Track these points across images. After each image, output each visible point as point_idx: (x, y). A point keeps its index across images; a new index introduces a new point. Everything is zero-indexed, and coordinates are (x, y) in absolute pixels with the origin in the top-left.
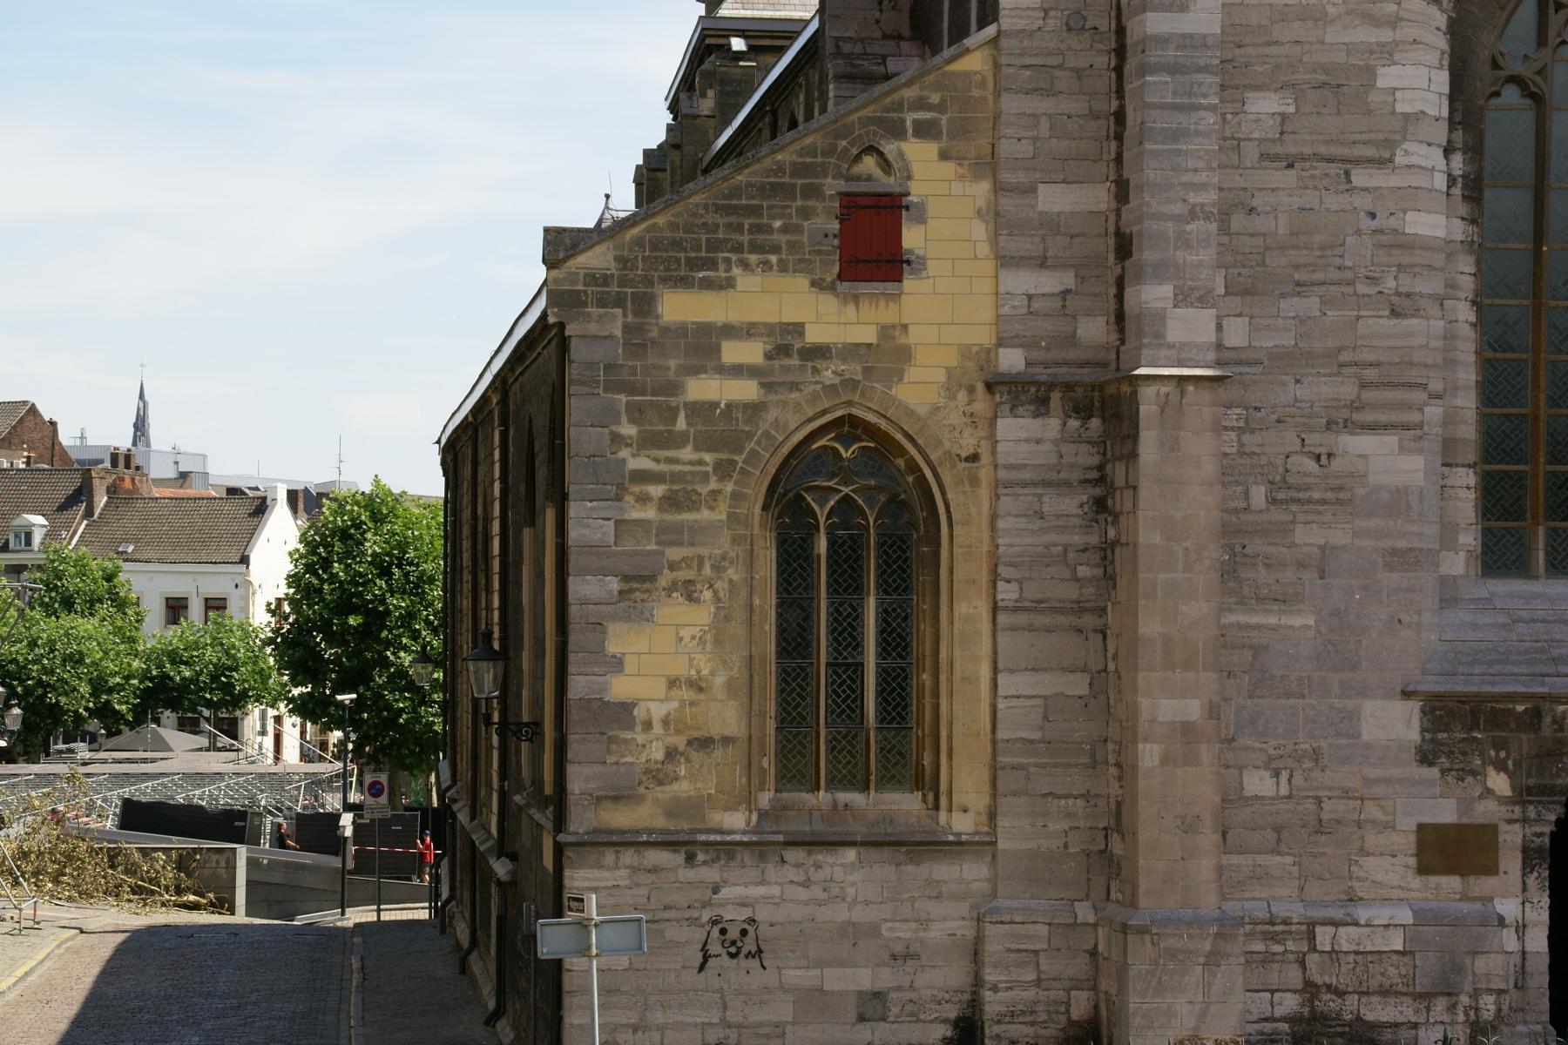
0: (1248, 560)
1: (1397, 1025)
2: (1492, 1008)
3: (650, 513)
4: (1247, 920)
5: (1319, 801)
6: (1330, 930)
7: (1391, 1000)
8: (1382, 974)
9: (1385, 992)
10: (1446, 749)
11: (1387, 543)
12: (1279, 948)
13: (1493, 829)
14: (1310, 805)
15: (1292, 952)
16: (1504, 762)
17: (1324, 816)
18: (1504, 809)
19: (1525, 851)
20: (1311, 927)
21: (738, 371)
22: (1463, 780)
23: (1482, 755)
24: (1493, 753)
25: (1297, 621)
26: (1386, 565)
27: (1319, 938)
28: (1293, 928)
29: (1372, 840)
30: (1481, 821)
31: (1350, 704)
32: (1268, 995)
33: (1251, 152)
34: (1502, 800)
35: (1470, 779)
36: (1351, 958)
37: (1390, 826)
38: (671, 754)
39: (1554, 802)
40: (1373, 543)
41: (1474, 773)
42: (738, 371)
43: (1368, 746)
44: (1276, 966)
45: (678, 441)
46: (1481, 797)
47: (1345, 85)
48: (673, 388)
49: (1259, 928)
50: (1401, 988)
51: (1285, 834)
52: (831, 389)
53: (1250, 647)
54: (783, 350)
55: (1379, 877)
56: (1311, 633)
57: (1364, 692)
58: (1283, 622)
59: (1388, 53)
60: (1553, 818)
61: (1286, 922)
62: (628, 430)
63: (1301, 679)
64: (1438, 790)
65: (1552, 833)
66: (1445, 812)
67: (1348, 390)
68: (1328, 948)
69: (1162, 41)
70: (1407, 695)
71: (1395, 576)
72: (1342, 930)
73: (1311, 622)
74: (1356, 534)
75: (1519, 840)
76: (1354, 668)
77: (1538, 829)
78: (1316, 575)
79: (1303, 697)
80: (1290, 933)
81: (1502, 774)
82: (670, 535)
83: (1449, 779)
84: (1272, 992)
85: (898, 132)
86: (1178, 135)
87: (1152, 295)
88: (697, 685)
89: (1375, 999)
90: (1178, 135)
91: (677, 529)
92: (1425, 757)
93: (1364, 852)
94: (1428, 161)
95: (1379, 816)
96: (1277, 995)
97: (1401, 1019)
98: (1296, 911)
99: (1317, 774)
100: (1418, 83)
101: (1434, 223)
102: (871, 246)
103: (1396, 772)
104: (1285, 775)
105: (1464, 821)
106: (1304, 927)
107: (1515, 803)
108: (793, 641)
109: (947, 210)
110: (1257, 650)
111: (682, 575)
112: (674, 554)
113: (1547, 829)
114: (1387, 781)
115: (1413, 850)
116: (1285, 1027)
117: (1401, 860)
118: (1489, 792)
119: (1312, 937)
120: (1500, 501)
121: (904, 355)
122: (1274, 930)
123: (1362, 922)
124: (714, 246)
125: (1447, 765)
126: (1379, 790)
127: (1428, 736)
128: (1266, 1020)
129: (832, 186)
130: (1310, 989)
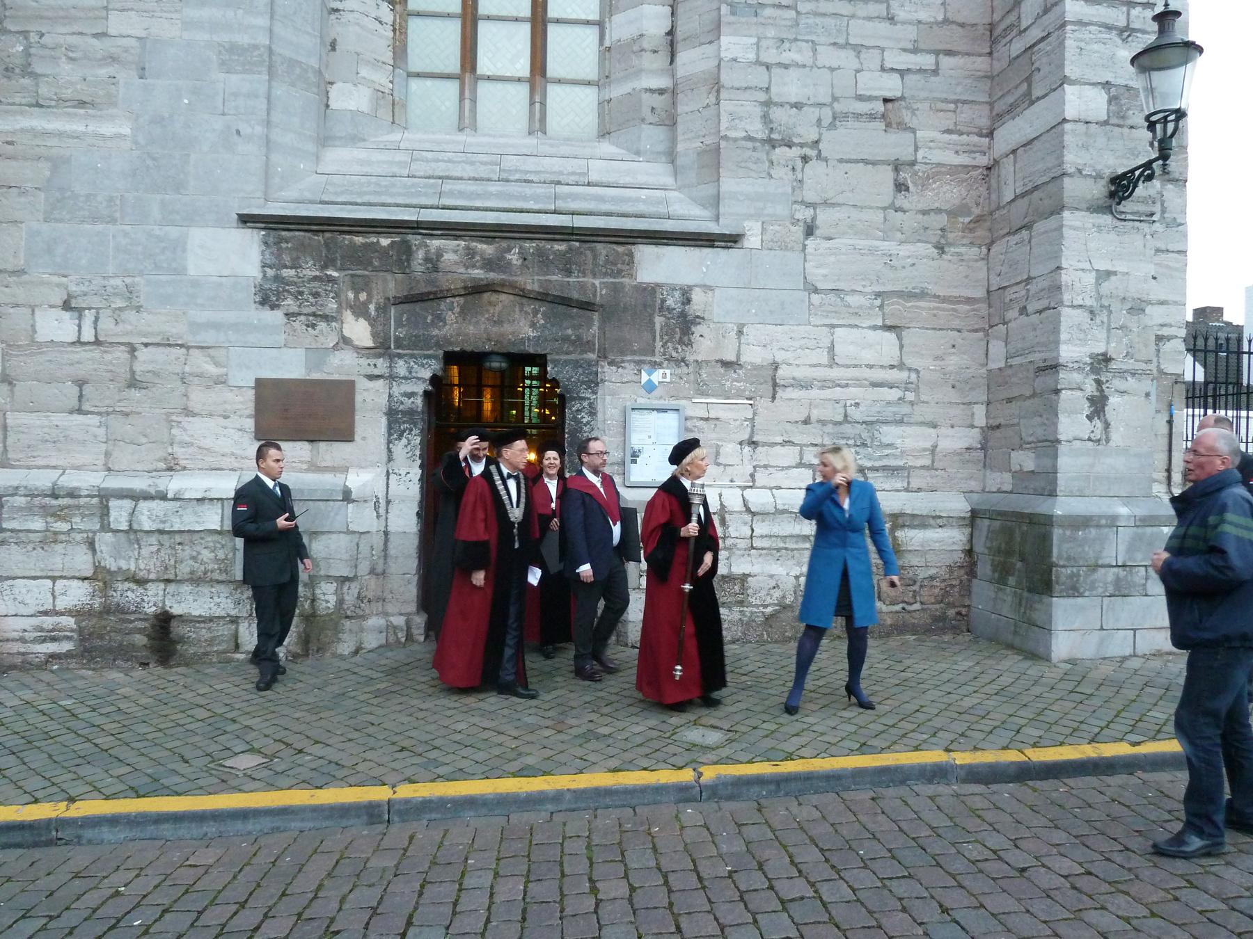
0: (47, 52)
1: (211, 619)
2: (333, 599)
4: (22, 491)
5: (132, 349)
6: (128, 504)
7: (205, 590)
8: (194, 558)
9: (196, 580)
10: (293, 289)
11: (225, 38)
12: (63, 526)
13: (348, 388)
14: (121, 354)
15: (81, 531)
16: (365, 304)
17: (138, 368)
18: (364, 362)
19: (391, 414)
20: (105, 497)
22: (313, 326)
23: (337, 296)
24: (351, 295)
25: (107, 129)
26: (223, 63)
27: (113, 514)
28: (82, 501)
29: (198, 398)
30: (336, 377)
31: (174, 232)
32: (49, 583)
34: (362, 351)
35: (322, 325)
36: (153, 539)
37: (221, 381)
39: (429, 357)
40: (207, 37)
41: (326, 318)
43: (195, 283)
44: (59, 548)
46: (336, 347)
49: (37, 501)
50: (216, 576)
51: (87, 389)
53: (47, 159)
55: (207, 443)
56: (127, 145)
57: (192, 218)
58: (90, 128)
60: (427, 374)
61: (72, 494)
63: (111, 199)
64: (281, 338)
65: (426, 394)
66: (290, 366)
68: (124, 527)
70: (246, 220)
71: (234, 78)
72: (144, 505)
73: (126, 130)
74: (188, 25)
75: (383, 401)
76: (179, 187)
77: (408, 387)
78: (134, 74)
79: (113, 221)
80: (78, 507)
81: (361, 320)
83: (297, 325)
84: (54, 579)
89: (186, 588)
92: (267, 300)
93: (188, 412)
95: (212, 369)
96: (60, 583)
97: (219, 612)
98: (87, 480)
99: (130, 315)
103: (230, 316)
104: (89, 317)
105: (316, 376)
106: (95, 501)
107: (379, 356)
110: (58, 163)
113: (420, 388)
114: (217, 326)
115: (250, 408)
116: (69, 622)
117: (235, 421)
118: (346, 341)
119: (105, 511)
122: (57, 502)
123: (170, 495)
125: (294, 309)
126: (208, 338)
127: (270, 272)
128: (46, 613)
130: (101, 577)
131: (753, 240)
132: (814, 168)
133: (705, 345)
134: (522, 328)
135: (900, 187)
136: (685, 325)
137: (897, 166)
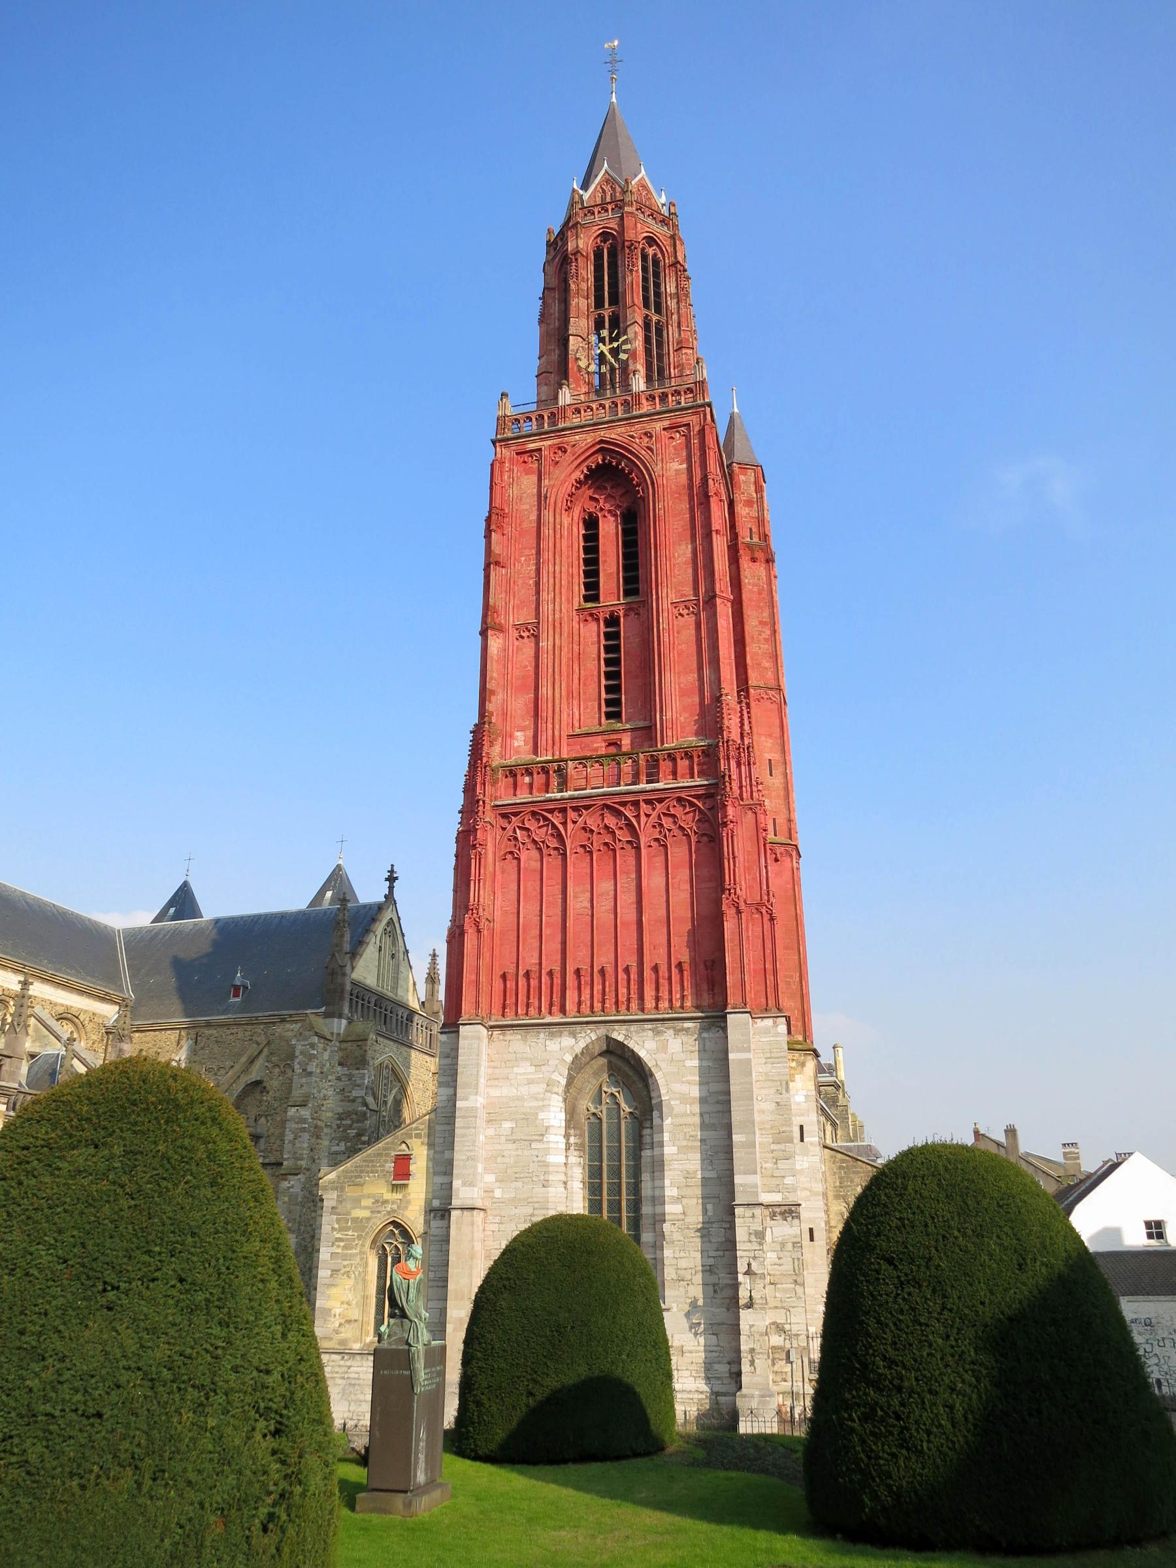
3: (339, 1251)
21: (365, 1208)
33: (503, 1139)
38: (340, 1325)
42: (365, 1208)
45: (348, 1229)
47: (529, 1119)
48: (348, 1213)
52: (389, 1213)
54: (377, 1201)
59: (543, 1108)
62: (336, 1226)
67: (530, 1211)
69: (461, 1109)
82: (345, 1257)
85: (411, 1138)
86: (464, 1136)
87: (456, 1183)
88: (348, 1304)
90: (464, 1136)
91: (346, 1255)
100: (555, 1116)
111: (347, 1269)
112: (345, 1263)
121: (408, 1202)
124: (362, 1172)
129: (393, 1153)
131: (675, 1309)
132: (691, 1287)
135: (715, 1291)
137: (714, 1285)
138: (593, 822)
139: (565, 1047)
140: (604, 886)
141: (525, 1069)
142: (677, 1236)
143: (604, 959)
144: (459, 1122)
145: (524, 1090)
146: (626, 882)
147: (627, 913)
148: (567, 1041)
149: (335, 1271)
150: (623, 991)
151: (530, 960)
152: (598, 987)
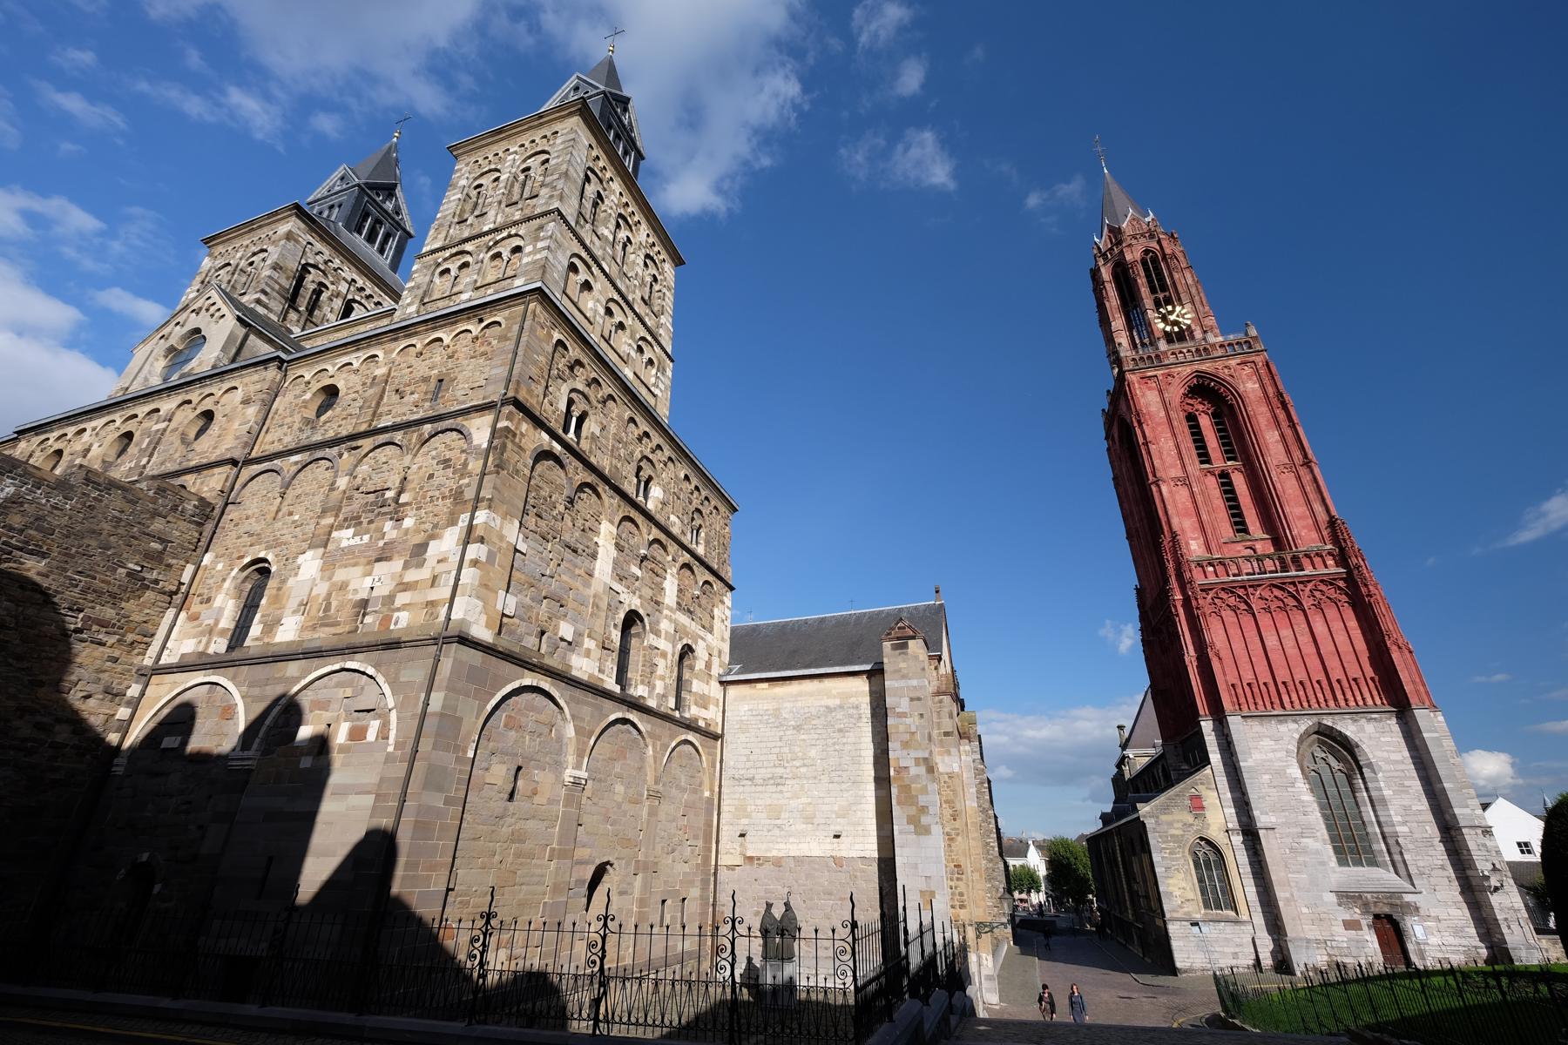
47: (1280, 773)
66: (1348, 917)
87: (1256, 813)
94: (1302, 787)
100: (1296, 772)
101: (1308, 798)
102: (1197, 805)
108: (1201, 880)
109: (1210, 798)
120: (1337, 851)
133: (1422, 912)
134: (1387, 910)
136: (1417, 909)
138: (1266, 594)
139: (1292, 730)
140: (1286, 633)
141: (1267, 743)
142: (1411, 846)
143: (1300, 675)
144: (1245, 775)
145: (1271, 755)
146: (1301, 627)
147: (1309, 649)
148: (1293, 726)
149: (1167, 869)
150: (1320, 696)
151: (1248, 676)
152: (1302, 693)
